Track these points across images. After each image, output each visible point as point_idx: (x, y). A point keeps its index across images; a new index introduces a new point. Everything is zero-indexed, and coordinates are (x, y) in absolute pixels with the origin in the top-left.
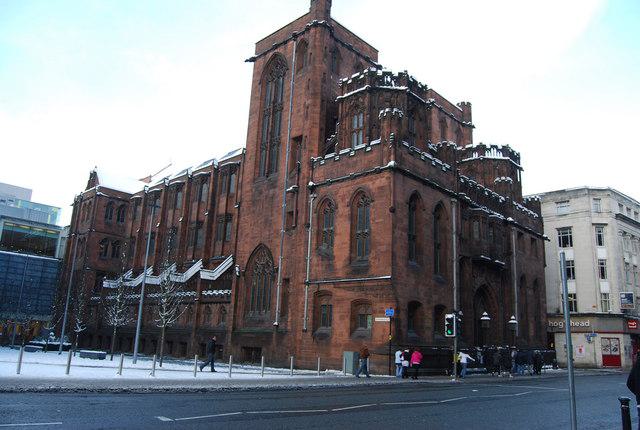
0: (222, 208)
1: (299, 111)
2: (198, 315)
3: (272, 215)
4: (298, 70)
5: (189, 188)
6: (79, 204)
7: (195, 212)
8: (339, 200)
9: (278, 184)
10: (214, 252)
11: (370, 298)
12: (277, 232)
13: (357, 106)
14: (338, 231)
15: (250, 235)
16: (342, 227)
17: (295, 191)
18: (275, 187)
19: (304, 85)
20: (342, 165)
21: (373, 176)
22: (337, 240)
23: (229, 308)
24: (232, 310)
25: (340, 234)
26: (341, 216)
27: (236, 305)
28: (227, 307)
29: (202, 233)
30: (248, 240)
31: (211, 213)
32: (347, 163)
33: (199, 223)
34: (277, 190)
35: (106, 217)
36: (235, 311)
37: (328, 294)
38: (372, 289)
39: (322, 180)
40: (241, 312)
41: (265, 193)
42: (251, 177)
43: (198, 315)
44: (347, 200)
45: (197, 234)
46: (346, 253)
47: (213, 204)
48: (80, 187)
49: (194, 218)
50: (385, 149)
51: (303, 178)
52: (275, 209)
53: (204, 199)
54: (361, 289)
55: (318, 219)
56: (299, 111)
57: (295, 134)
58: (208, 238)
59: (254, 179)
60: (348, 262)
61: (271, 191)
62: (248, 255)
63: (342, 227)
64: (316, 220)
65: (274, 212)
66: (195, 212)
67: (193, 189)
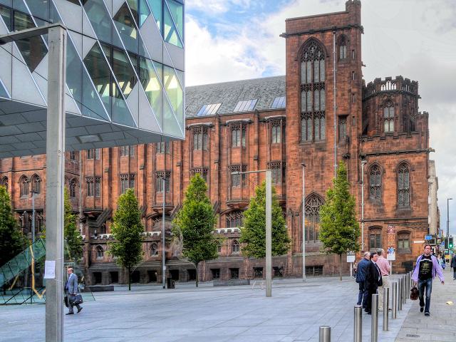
1: (343, 95)
3: (323, 172)
4: (338, 61)
8: (386, 167)
9: (328, 148)
11: (410, 229)
13: (389, 100)
14: (386, 188)
16: (389, 186)
17: (347, 157)
18: (325, 151)
19: (347, 75)
20: (388, 143)
21: (413, 155)
22: (386, 194)
25: (389, 189)
26: (388, 178)
32: (392, 143)
34: (326, 153)
37: (379, 228)
38: (413, 224)
39: (370, 151)
41: (314, 154)
44: (393, 168)
46: (394, 202)
50: (423, 137)
51: (354, 148)
52: (326, 168)
54: (405, 224)
55: (368, 178)
56: (343, 95)
57: (341, 112)
60: (395, 208)
61: (320, 154)
63: (389, 186)
64: (367, 180)
65: (325, 170)
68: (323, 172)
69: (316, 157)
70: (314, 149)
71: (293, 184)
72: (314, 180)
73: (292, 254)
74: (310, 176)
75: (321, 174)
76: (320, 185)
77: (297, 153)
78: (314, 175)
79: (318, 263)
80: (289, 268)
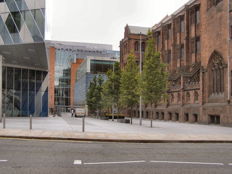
0: (193, 35)
2: (183, 98)
5: (174, 25)
6: (123, 45)
7: (178, 39)
10: (191, 61)
12: (225, 40)
15: (208, 46)
18: (221, 11)
23: (200, 92)
24: (201, 93)
27: (203, 91)
28: (198, 92)
29: (184, 50)
30: (207, 49)
31: (188, 38)
33: (182, 46)
34: (223, 12)
35: (135, 50)
36: (203, 94)
40: (207, 94)
41: (215, 17)
42: (205, 8)
43: (183, 98)
45: (181, 51)
47: (188, 33)
48: (122, 36)
49: (178, 42)
53: (183, 30)
58: (188, 52)
59: (208, 10)
61: (219, 15)
62: (208, 59)
66: (178, 39)
67: (176, 26)
68: (221, 30)
69: (216, 19)
70: (215, 12)
71: (204, 46)
72: (216, 40)
73: (203, 104)
74: (213, 36)
75: (220, 33)
76: (219, 43)
77: (206, 20)
78: (215, 35)
79: (217, 113)
80: (201, 115)
